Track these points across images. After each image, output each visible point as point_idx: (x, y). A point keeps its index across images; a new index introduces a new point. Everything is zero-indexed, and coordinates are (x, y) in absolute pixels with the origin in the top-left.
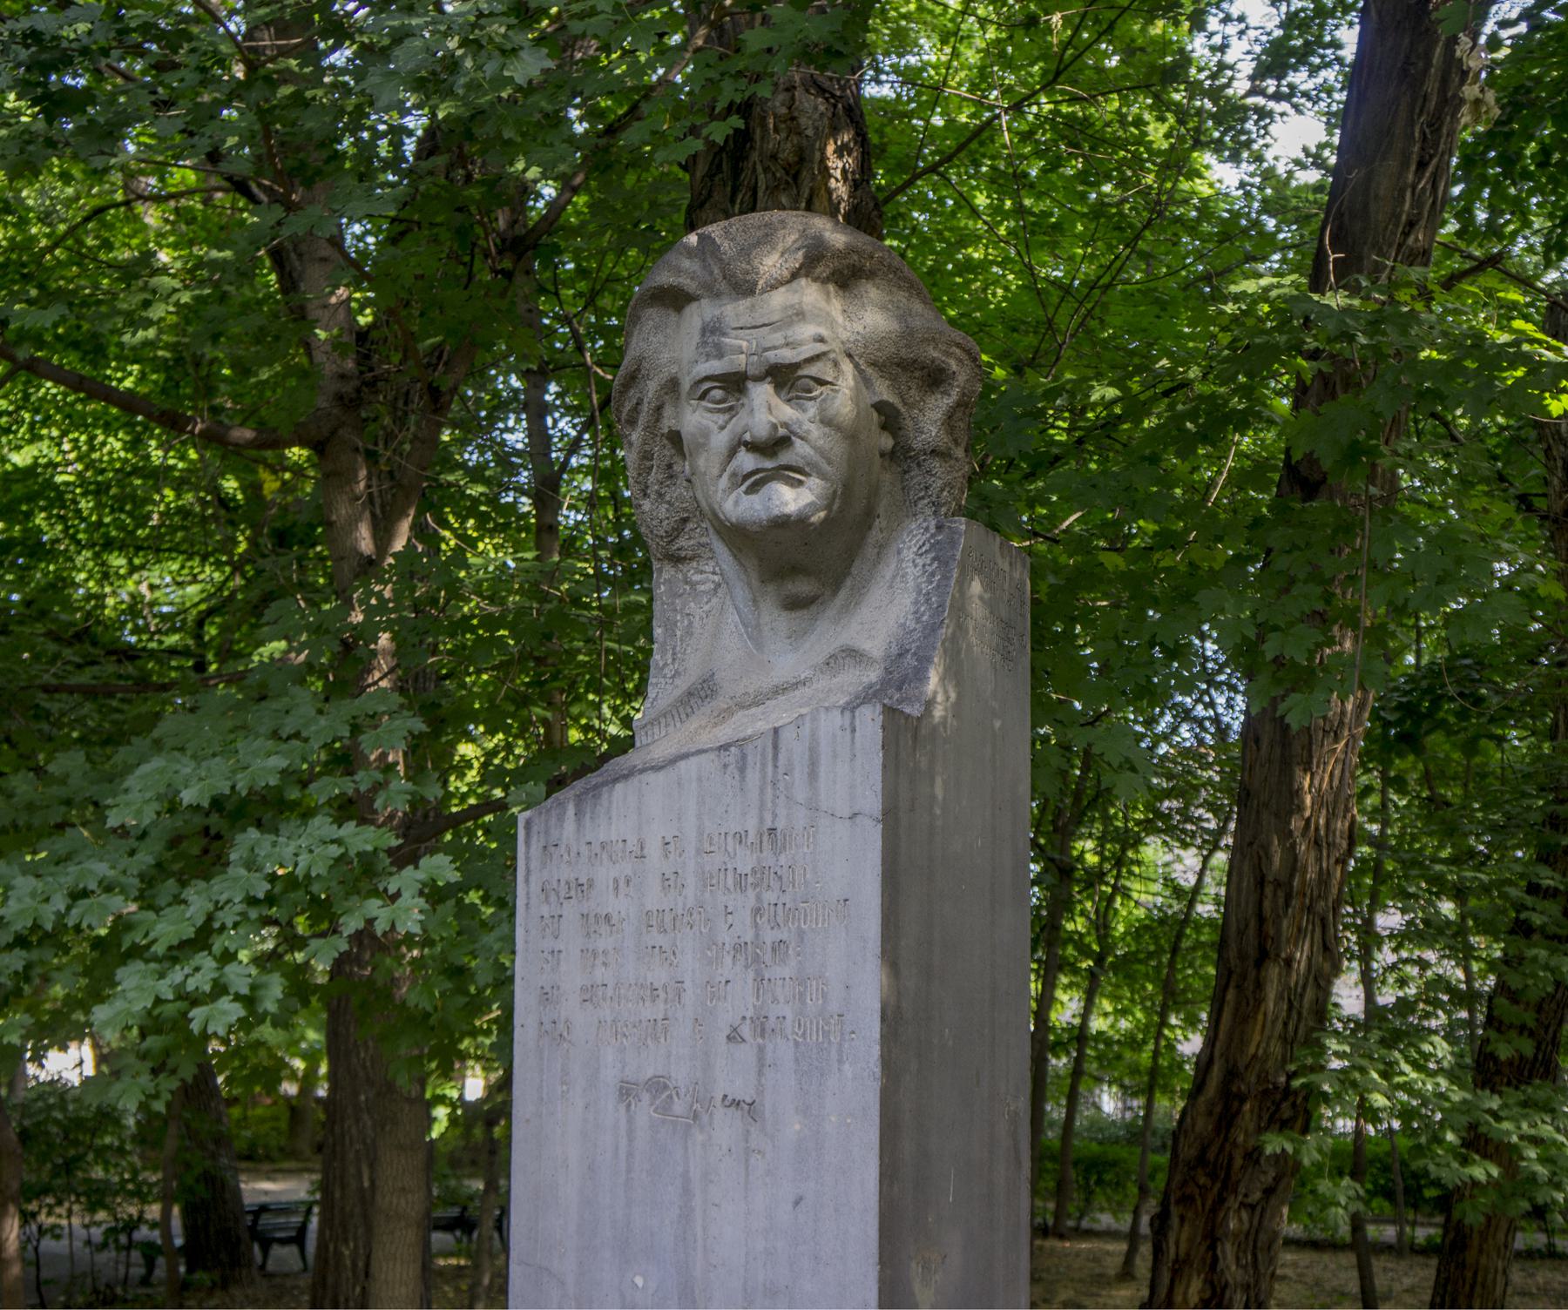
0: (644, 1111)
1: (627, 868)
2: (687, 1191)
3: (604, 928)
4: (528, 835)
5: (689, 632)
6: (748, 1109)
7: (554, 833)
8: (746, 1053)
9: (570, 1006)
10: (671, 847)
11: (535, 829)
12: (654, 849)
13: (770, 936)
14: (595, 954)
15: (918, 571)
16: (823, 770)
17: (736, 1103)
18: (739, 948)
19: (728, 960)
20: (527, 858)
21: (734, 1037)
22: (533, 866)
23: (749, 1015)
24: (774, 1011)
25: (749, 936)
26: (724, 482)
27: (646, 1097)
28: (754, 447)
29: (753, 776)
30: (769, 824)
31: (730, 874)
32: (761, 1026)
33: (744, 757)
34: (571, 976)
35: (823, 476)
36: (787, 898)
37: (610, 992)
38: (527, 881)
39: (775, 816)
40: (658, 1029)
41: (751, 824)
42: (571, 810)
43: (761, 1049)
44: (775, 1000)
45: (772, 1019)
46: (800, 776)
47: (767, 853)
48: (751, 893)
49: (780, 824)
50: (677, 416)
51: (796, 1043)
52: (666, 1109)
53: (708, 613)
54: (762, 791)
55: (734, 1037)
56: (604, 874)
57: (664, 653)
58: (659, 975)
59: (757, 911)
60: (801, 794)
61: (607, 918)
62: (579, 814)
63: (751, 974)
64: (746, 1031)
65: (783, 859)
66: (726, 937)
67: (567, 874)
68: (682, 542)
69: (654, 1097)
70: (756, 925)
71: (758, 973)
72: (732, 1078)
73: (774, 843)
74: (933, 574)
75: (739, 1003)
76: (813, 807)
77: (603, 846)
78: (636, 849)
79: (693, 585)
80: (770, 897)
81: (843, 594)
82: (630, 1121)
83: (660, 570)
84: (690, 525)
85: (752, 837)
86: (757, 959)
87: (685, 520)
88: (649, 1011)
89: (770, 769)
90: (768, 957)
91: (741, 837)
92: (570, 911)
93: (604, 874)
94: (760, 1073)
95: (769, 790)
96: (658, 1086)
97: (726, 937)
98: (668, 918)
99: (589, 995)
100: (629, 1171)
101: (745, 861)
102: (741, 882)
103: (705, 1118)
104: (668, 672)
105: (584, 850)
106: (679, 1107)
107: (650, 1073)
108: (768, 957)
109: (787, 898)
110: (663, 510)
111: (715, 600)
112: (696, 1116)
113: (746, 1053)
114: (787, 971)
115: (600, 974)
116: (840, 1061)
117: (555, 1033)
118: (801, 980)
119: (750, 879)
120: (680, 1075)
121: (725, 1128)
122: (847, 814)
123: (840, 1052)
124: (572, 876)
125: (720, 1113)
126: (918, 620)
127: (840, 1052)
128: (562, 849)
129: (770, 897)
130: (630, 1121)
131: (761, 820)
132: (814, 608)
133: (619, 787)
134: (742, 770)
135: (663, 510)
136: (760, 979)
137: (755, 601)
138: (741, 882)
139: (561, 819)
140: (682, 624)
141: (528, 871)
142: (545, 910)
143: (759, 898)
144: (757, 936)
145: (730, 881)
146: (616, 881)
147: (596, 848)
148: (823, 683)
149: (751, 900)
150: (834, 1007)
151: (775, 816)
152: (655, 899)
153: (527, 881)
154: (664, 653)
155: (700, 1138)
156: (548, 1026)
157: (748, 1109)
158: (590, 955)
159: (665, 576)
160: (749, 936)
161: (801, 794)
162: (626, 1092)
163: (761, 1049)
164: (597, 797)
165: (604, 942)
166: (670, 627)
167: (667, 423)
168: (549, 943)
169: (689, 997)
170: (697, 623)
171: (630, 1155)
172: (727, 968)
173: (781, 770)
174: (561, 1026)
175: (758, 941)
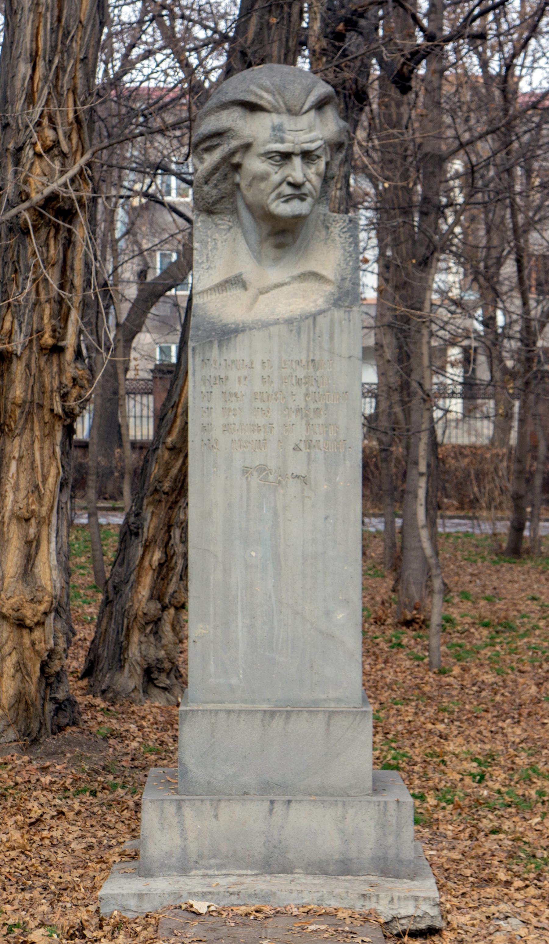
0: (255, 481)
2: (276, 514)
3: (234, 399)
4: (194, 354)
5: (215, 248)
6: (304, 480)
7: (208, 355)
8: (302, 455)
9: (217, 433)
10: (266, 365)
11: (197, 351)
12: (258, 366)
13: (312, 406)
14: (230, 410)
15: (343, 240)
16: (336, 336)
17: (297, 477)
18: (298, 410)
19: (293, 415)
20: (194, 365)
21: (297, 448)
22: (197, 368)
23: (303, 439)
24: (315, 438)
25: (303, 406)
26: (274, 195)
27: (256, 474)
28: (290, 184)
29: (304, 337)
30: (311, 357)
31: (294, 378)
32: (309, 444)
33: (300, 328)
34: (218, 419)
35: (313, 197)
36: (320, 390)
37: (237, 427)
38: (194, 375)
39: (314, 354)
40: (261, 444)
41: (303, 357)
42: (216, 345)
43: (309, 454)
44: (315, 433)
45: (314, 441)
46: (326, 337)
47: (311, 370)
48: (303, 387)
49: (317, 358)
50: (243, 158)
51: (325, 452)
52: (265, 479)
53: (225, 240)
54: (308, 343)
55: (297, 448)
56: (234, 374)
57: (201, 256)
58: (260, 420)
59: (307, 395)
60: (326, 346)
61: (236, 395)
62: (220, 346)
63: (304, 422)
64: (302, 446)
65: (318, 373)
66: (293, 406)
67: (213, 373)
68: (218, 206)
69: (260, 474)
70: (306, 401)
71: (307, 421)
72: (296, 464)
73: (314, 366)
74: (351, 243)
75: (299, 432)
76: (331, 352)
77: (233, 362)
78: (249, 364)
80: (312, 389)
81: (298, 242)
82: (248, 484)
84: (225, 200)
85: (304, 363)
86: (307, 416)
87: (223, 197)
88: (256, 436)
89: (312, 334)
90: (312, 415)
91: (298, 362)
92: (216, 390)
93: (234, 374)
94: (309, 464)
95: (312, 343)
96: (262, 469)
97: (293, 406)
98: (265, 396)
99: (227, 428)
100: (248, 506)
101: (301, 373)
102: (298, 382)
103: (284, 483)
104: (205, 266)
105: (223, 363)
106: (271, 478)
107: (258, 463)
108: (312, 415)
109: (320, 390)
111: (228, 234)
112: (279, 482)
113: (302, 455)
114: (320, 421)
115: (232, 419)
116: (344, 460)
117: (209, 445)
118: (327, 425)
119: (303, 381)
120: (272, 464)
121: (293, 487)
122: (347, 356)
123: (344, 455)
124: (217, 374)
125: (291, 481)
126: (347, 264)
127: (344, 455)
128: (212, 361)
129: (312, 389)
130: (248, 484)
131: (308, 356)
133: (241, 336)
134: (299, 333)
135: (215, 192)
136: (308, 424)
138: (298, 382)
139: (211, 348)
141: (194, 371)
142: (203, 389)
143: (307, 389)
144: (307, 406)
145: (294, 382)
146: (239, 378)
147: (229, 362)
148: (296, 285)
149: (304, 391)
150: (342, 437)
151: (314, 354)
152: (258, 387)
153: (194, 375)
155: (281, 491)
156: (206, 441)
157: (304, 480)
158: (226, 410)
160: (303, 406)
161: (326, 346)
162: (246, 471)
163: (309, 454)
164: (229, 339)
165: (234, 404)
166: (204, 243)
167: (236, 159)
168: (206, 404)
169: (275, 431)
170: (219, 244)
171: (248, 499)
172: (293, 419)
173: (317, 335)
174: (213, 442)
175: (307, 408)
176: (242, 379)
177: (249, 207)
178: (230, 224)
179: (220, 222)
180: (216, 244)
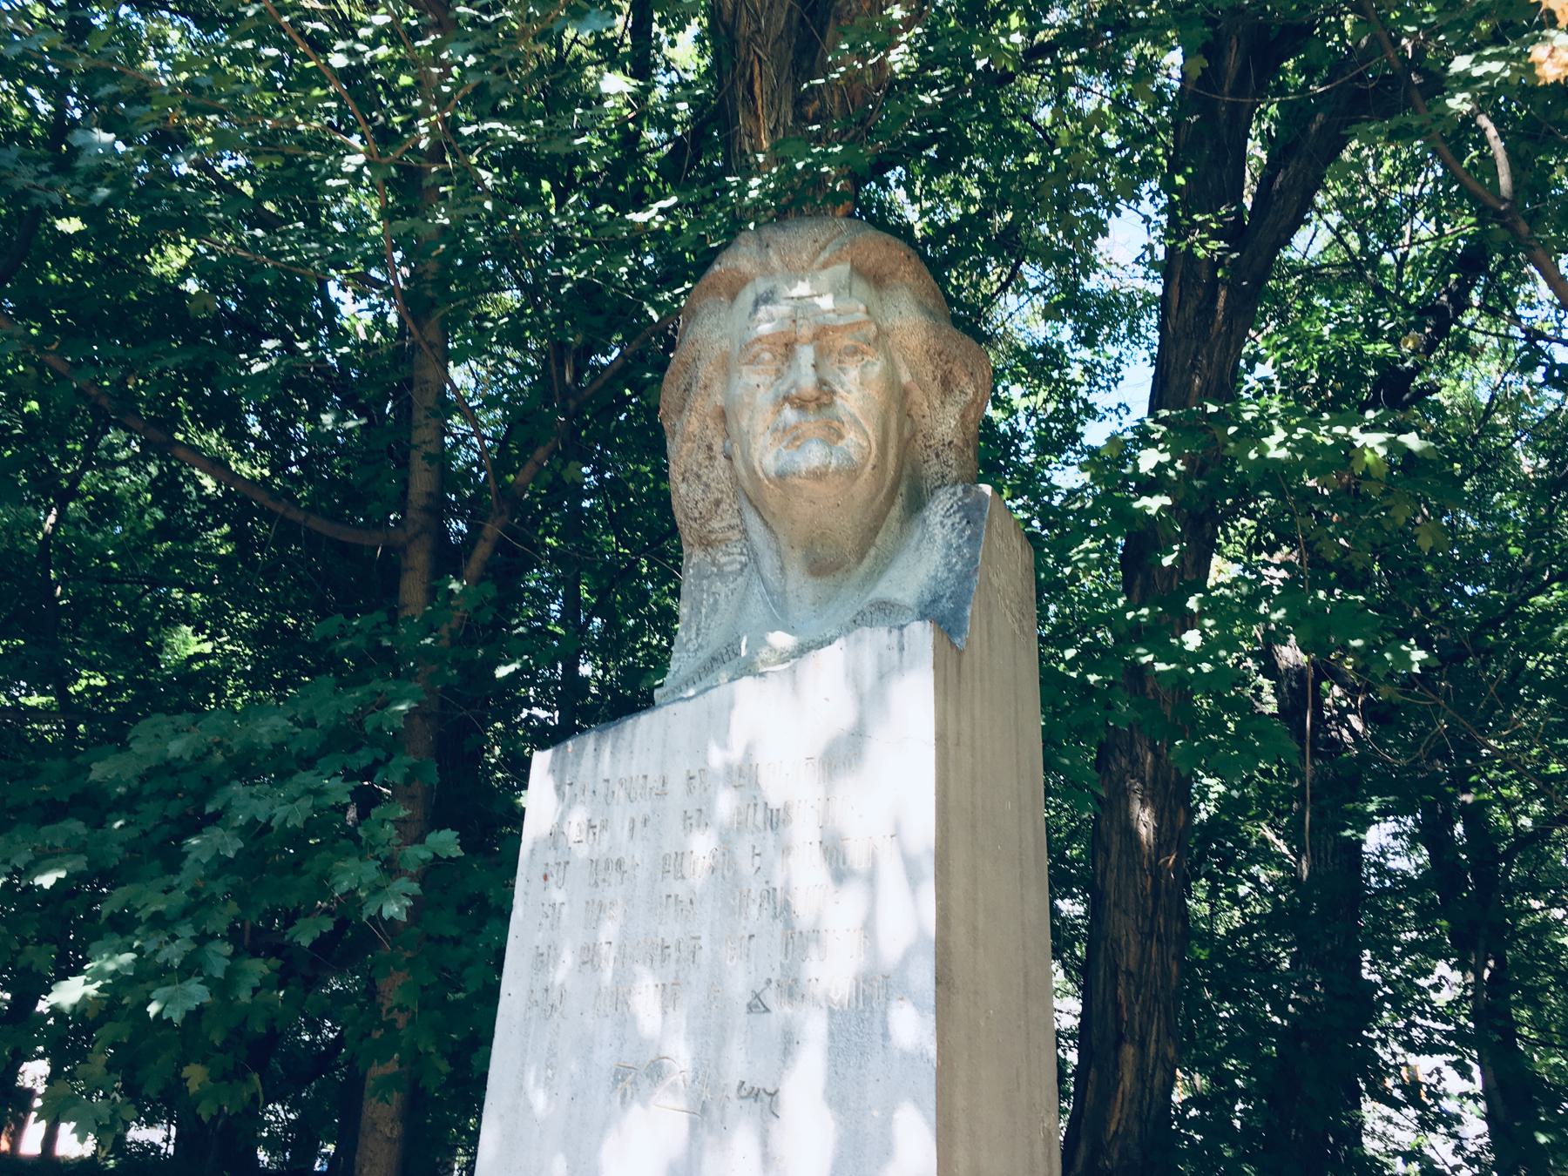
1: (645, 806)
3: (614, 877)
5: (714, 608)
10: (696, 782)
12: (677, 785)
17: (755, 1094)
23: (774, 977)
58: (671, 930)
68: (715, 524)
79: (720, 567)
83: (690, 556)
110: (699, 495)
111: (740, 579)
132: (839, 575)
137: (782, 569)
140: (707, 600)
146: (633, 821)
154: (687, 628)
156: (538, 996)
159: (694, 560)
166: (696, 609)
170: (722, 601)
174: (554, 996)
176: (639, 825)
177: (750, 501)
178: (743, 559)
179: (723, 560)
180: (716, 601)
